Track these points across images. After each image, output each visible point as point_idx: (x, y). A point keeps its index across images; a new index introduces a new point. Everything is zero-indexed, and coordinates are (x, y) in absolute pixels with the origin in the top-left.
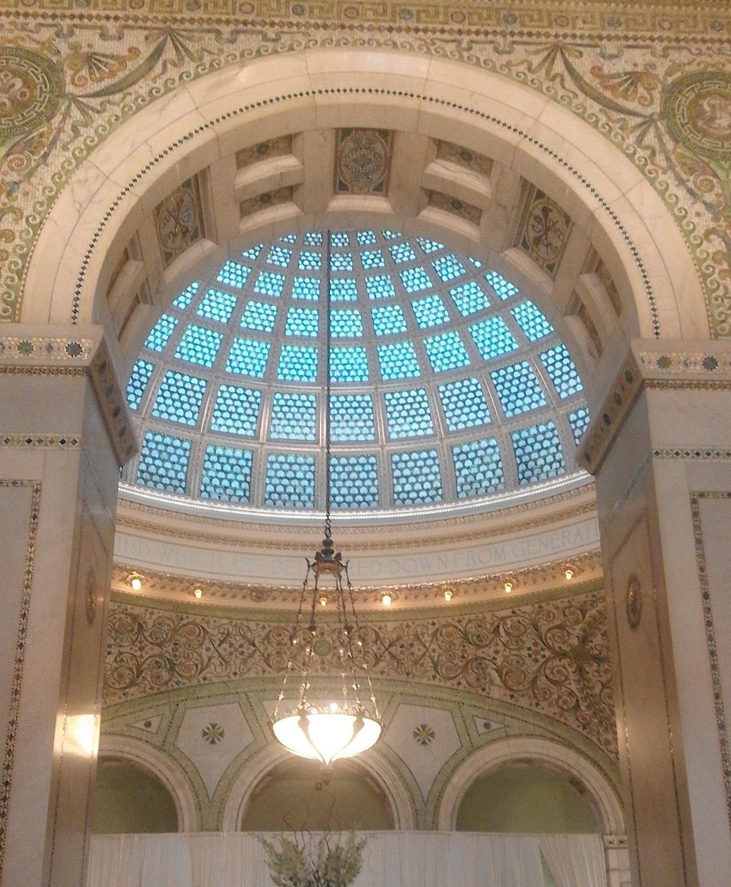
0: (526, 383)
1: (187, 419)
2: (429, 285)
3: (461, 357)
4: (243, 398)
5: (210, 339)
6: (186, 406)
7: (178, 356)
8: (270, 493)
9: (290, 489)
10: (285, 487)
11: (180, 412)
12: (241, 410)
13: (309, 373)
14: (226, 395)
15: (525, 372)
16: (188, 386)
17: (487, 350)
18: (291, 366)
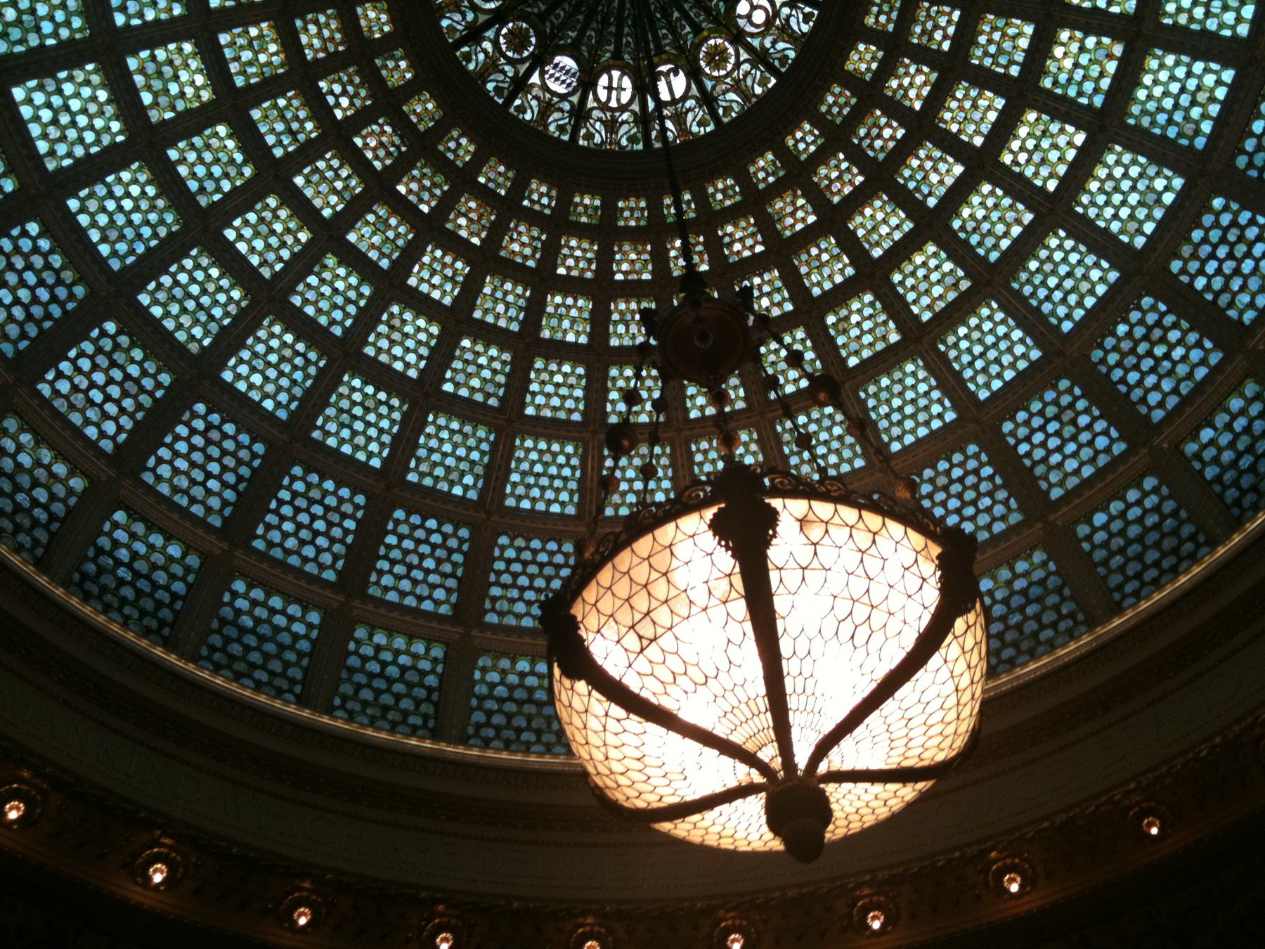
0: (975, 487)
1: (322, 567)
2: (789, 307)
3: (847, 454)
4: (436, 538)
5: (384, 410)
6: (322, 542)
7: (316, 434)
8: (478, 726)
9: (521, 722)
10: (509, 716)
11: (309, 551)
12: (429, 563)
13: (564, 496)
14: (404, 529)
15: (972, 464)
16: (331, 501)
17: (896, 431)
18: (531, 480)
